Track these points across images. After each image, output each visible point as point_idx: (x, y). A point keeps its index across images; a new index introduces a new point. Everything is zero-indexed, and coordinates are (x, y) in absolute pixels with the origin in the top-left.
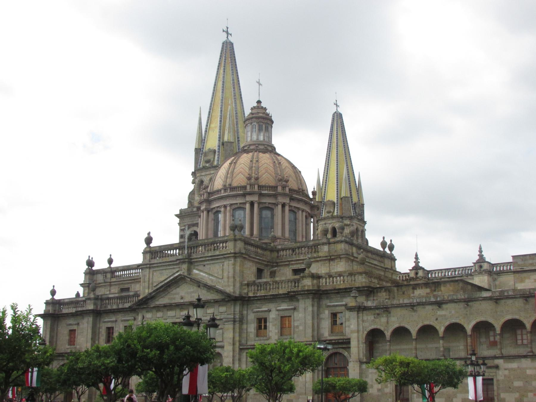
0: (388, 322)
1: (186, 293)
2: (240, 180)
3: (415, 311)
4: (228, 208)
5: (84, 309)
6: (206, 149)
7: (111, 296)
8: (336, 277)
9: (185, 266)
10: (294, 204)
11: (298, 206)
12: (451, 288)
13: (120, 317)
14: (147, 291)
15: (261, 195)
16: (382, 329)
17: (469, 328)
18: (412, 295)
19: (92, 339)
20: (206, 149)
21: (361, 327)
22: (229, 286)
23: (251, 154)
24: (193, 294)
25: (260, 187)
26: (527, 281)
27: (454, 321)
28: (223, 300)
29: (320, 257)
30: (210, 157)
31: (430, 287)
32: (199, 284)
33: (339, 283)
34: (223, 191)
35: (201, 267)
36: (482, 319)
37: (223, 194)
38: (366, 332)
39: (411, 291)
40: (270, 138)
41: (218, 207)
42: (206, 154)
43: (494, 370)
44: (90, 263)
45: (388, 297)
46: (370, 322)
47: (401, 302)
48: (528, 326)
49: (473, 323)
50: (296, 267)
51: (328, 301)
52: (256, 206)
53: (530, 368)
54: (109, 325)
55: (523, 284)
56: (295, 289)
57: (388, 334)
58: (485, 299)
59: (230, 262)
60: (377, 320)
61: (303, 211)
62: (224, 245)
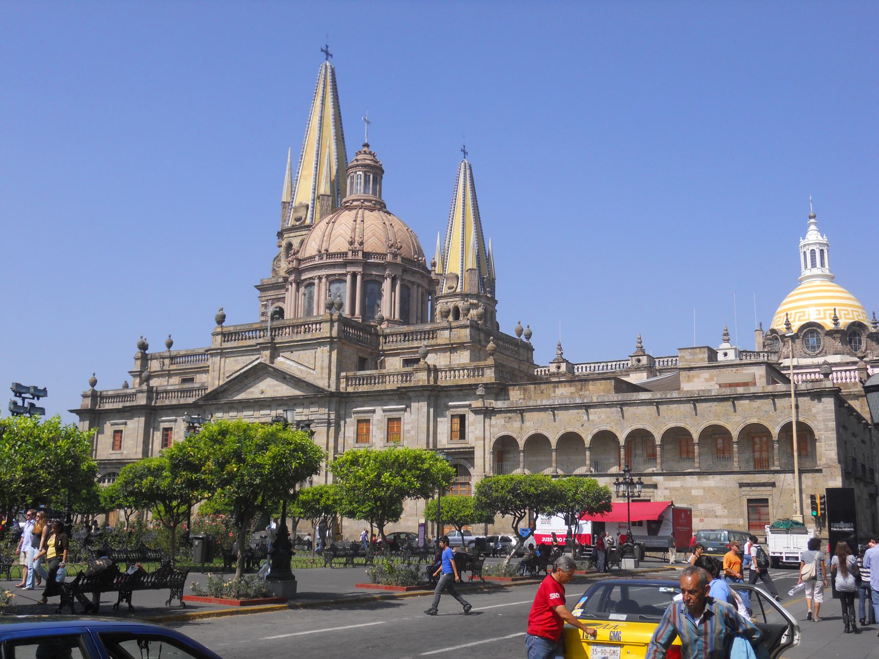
0: (521, 428)
1: (269, 388)
2: (339, 244)
4: (324, 280)
5: (134, 404)
6: (296, 203)
7: (169, 388)
8: (459, 370)
9: (267, 353)
10: (408, 277)
11: (413, 279)
14: (217, 383)
15: (366, 265)
16: (514, 436)
17: (622, 438)
18: (553, 395)
19: (144, 442)
20: (296, 203)
21: (487, 434)
22: (322, 378)
23: (354, 212)
24: (276, 388)
25: (366, 255)
26: (695, 380)
27: (603, 428)
28: (315, 396)
29: (439, 345)
30: (302, 213)
33: (463, 379)
34: (317, 258)
35: (287, 354)
36: (640, 426)
37: (317, 261)
38: (494, 440)
39: (552, 390)
41: (310, 278)
42: (296, 209)
43: (652, 490)
44: (143, 347)
45: (522, 397)
46: (499, 427)
47: (539, 403)
48: (696, 436)
49: (628, 431)
50: (407, 357)
52: (359, 278)
54: (167, 425)
55: (690, 384)
56: (407, 385)
57: (521, 443)
58: (644, 403)
59: (325, 348)
60: (508, 425)
61: (418, 286)
62: (318, 326)
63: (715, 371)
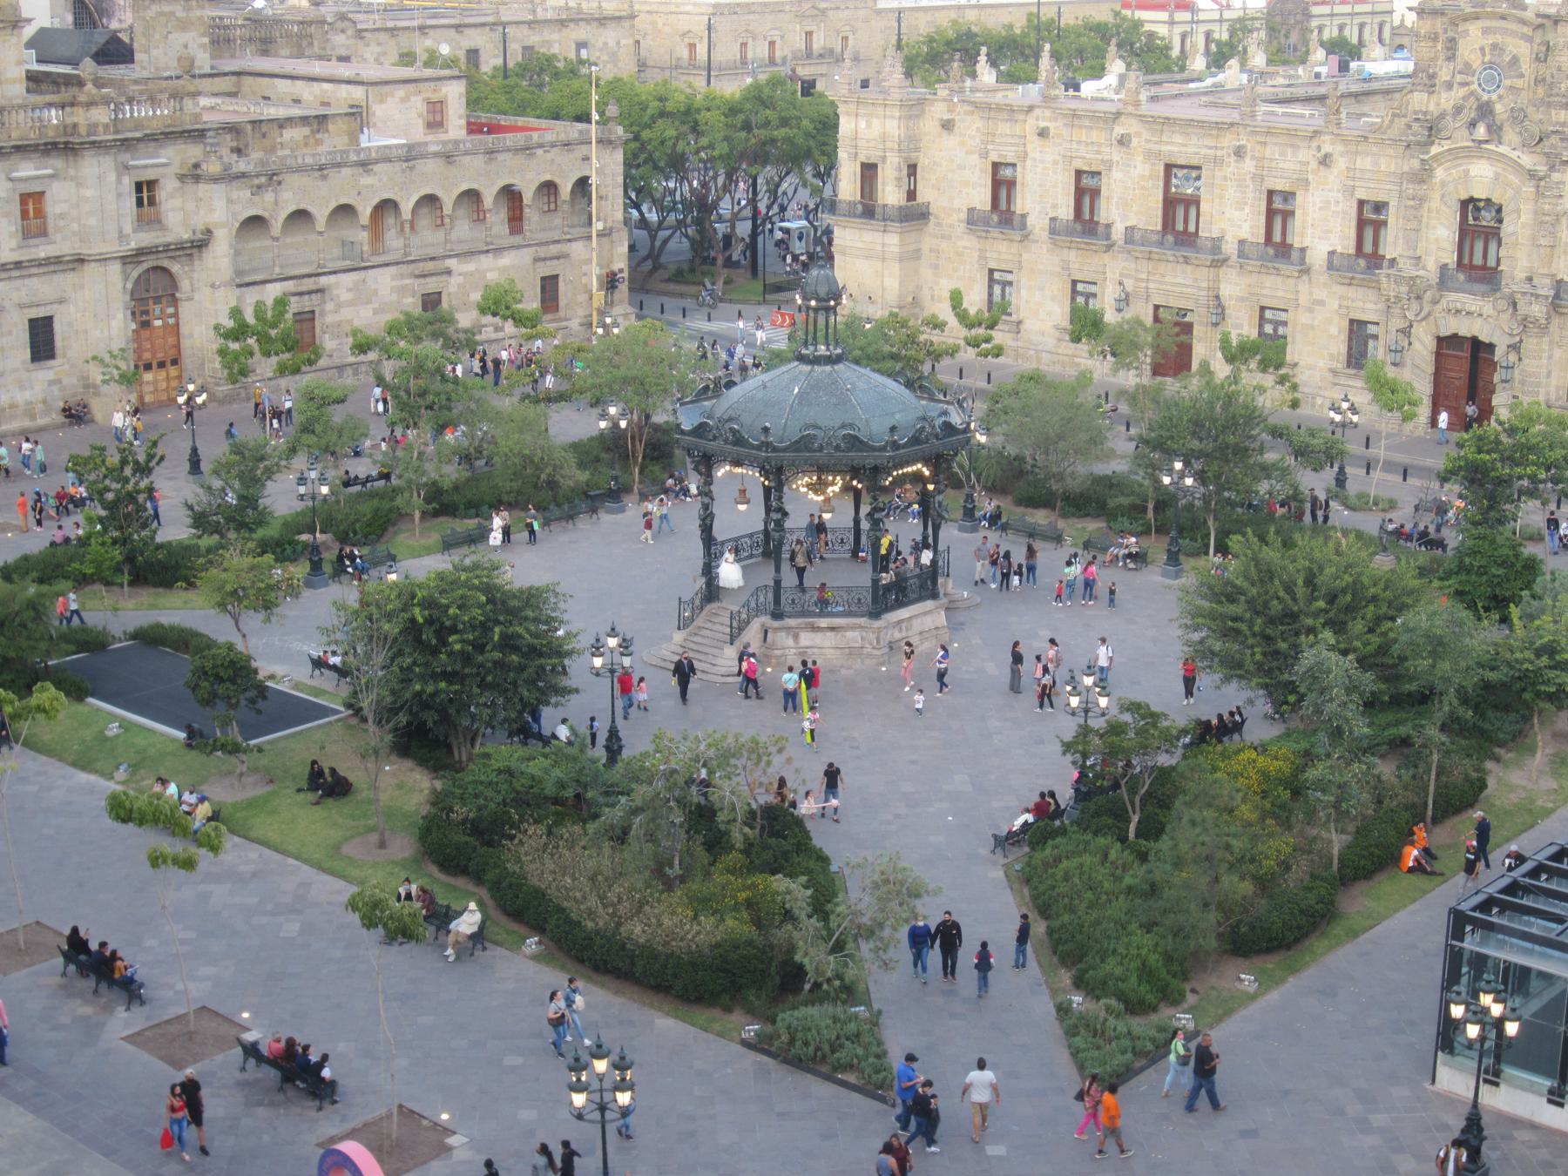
0: (276, 203)
3: (324, 177)
12: (345, 127)
16: (266, 215)
31: (309, 124)
43: (444, 278)
51: (128, 156)
53: (491, 270)
60: (256, 199)
63: (411, 87)
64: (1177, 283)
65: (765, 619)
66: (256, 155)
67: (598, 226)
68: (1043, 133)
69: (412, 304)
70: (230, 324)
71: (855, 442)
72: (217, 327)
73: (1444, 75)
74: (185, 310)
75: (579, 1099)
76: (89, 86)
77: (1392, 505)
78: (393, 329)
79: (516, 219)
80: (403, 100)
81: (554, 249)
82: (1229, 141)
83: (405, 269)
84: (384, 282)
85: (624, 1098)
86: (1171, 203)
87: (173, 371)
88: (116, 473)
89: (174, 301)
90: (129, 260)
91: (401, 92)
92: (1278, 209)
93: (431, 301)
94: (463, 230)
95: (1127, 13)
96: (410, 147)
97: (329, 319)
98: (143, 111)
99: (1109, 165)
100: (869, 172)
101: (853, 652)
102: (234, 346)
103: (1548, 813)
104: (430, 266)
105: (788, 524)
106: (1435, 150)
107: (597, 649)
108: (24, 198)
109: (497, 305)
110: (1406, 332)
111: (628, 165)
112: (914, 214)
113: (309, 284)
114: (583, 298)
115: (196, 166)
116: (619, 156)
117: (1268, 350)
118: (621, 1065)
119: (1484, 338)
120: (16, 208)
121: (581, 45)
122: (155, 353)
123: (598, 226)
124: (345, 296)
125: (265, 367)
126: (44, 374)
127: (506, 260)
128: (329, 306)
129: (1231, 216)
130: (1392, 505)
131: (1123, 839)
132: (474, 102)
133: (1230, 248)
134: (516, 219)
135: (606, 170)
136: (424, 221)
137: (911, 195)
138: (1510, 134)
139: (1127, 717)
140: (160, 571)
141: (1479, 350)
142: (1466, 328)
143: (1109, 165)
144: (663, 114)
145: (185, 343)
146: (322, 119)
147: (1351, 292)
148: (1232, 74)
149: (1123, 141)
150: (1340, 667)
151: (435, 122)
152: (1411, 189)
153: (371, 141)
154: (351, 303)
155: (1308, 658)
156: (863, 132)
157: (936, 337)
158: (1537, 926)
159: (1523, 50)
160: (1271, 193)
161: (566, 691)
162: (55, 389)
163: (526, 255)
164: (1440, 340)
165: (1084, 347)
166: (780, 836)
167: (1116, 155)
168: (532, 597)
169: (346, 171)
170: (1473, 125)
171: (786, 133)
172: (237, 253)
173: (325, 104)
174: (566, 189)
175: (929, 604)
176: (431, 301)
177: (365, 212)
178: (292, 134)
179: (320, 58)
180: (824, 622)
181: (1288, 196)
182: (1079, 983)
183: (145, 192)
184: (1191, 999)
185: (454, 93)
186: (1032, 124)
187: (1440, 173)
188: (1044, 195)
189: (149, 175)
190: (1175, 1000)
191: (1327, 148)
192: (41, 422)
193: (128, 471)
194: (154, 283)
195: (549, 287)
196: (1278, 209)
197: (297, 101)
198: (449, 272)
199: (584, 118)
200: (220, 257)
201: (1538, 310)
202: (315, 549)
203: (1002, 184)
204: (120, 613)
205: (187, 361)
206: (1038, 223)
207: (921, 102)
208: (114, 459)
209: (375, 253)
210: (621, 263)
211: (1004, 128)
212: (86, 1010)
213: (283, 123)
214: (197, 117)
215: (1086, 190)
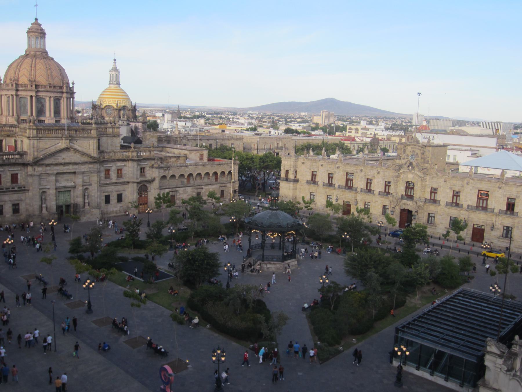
13: (6, 168)
32: (76, 151)
40: (45, 46)
64: (348, 196)
65: (260, 261)
66: (165, 163)
67: (233, 180)
68: (322, 165)
69: (195, 195)
70: (157, 197)
71: (280, 226)
72: (155, 197)
73: (403, 156)
74: (149, 193)
75: (214, 359)
76: (133, 148)
77: (390, 243)
78: (190, 199)
79: (216, 179)
80: (196, 154)
81: (224, 185)
82: (359, 168)
83: (194, 187)
84: (189, 190)
85: (223, 359)
86: (347, 180)
87: (146, 206)
88: (132, 226)
89: (147, 192)
90: (138, 183)
91: (195, 152)
92: (369, 182)
93: (199, 194)
94: (206, 180)
95: (342, 141)
96: (196, 163)
97: (178, 197)
98: (143, 154)
99: (335, 172)
100: (287, 172)
101: (278, 269)
102: (158, 201)
103: (419, 308)
104: (199, 187)
105: (266, 242)
106: (401, 171)
107: (226, 265)
108: (118, 170)
109: (211, 195)
110: (394, 208)
111: (239, 168)
112: (296, 181)
113: (174, 190)
114: (229, 195)
115: (153, 165)
116: (238, 167)
117: (366, 210)
118: (223, 352)
119: (410, 209)
120: (116, 172)
121: (232, 144)
122: (142, 201)
123: (233, 180)
124: (181, 192)
125: (164, 206)
126: (120, 205)
127: (214, 186)
128: (178, 194)
129: (359, 183)
130: (390, 243)
131: (330, 309)
132: (209, 155)
133: (359, 190)
134: (216, 179)
135: (235, 169)
136: (198, 178)
137: (295, 177)
138: (416, 169)
139: (332, 285)
140: (139, 245)
141: (410, 212)
142: (407, 207)
143: (335, 172)
144: (247, 159)
145: (148, 200)
146: (179, 157)
147: (383, 199)
148: (361, 155)
149: (338, 168)
150: (376, 276)
151: (201, 158)
152: (396, 179)
153: (188, 162)
154: (182, 194)
155: (369, 274)
156: (287, 164)
157: (298, 206)
158: (414, 332)
159: (419, 152)
160: (367, 179)
161: (219, 274)
162: (122, 208)
163: (218, 185)
164: (401, 210)
165: (329, 208)
166: (260, 306)
167: (336, 170)
168: (213, 255)
169: (183, 167)
170: (409, 166)
171: (272, 163)
172: (160, 183)
173: (180, 154)
174: (226, 173)
175: (294, 260)
176: (199, 194)
177: (186, 176)
178: (172, 160)
179: (179, 145)
180: (272, 262)
181: (371, 180)
182: (320, 340)
183: (142, 170)
184: (342, 344)
185: (205, 153)
186: (320, 163)
187: (402, 176)
188: (322, 178)
189: (143, 166)
190: (339, 344)
191: (379, 170)
192: (118, 214)
193: (135, 225)
194: (143, 188)
195: (222, 192)
196: (369, 182)
197: (174, 153)
198: (202, 188)
199: (231, 159)
200: (156, 184)
201: (421, 204)
202: (171, 243)
203: (314, 175)
204: (131, 254)
205: (149, 204)
206: (320, 184)
207: (298, 159)
208: (132, 223)
209: (188, 184)
210: (237, 188)
211: (315, 164)
212: (116, 335)
213: (171, 157)
214: (153, 155)
215: (330, 177)
